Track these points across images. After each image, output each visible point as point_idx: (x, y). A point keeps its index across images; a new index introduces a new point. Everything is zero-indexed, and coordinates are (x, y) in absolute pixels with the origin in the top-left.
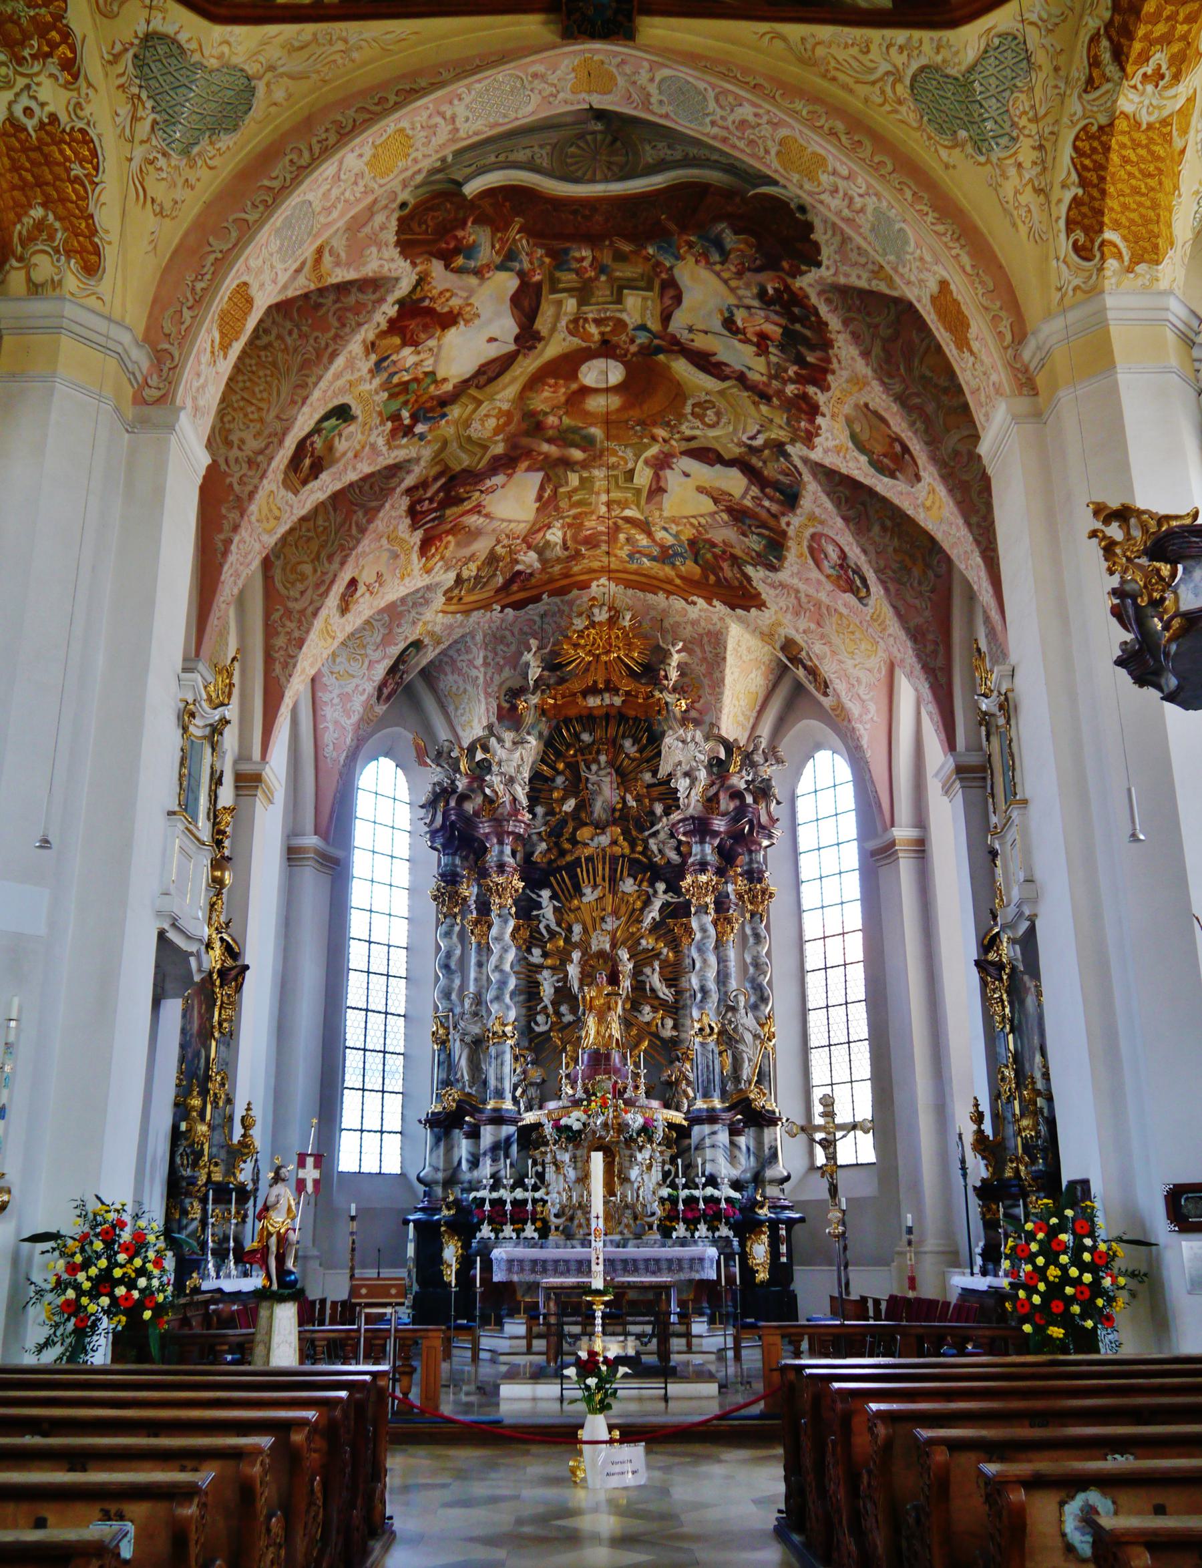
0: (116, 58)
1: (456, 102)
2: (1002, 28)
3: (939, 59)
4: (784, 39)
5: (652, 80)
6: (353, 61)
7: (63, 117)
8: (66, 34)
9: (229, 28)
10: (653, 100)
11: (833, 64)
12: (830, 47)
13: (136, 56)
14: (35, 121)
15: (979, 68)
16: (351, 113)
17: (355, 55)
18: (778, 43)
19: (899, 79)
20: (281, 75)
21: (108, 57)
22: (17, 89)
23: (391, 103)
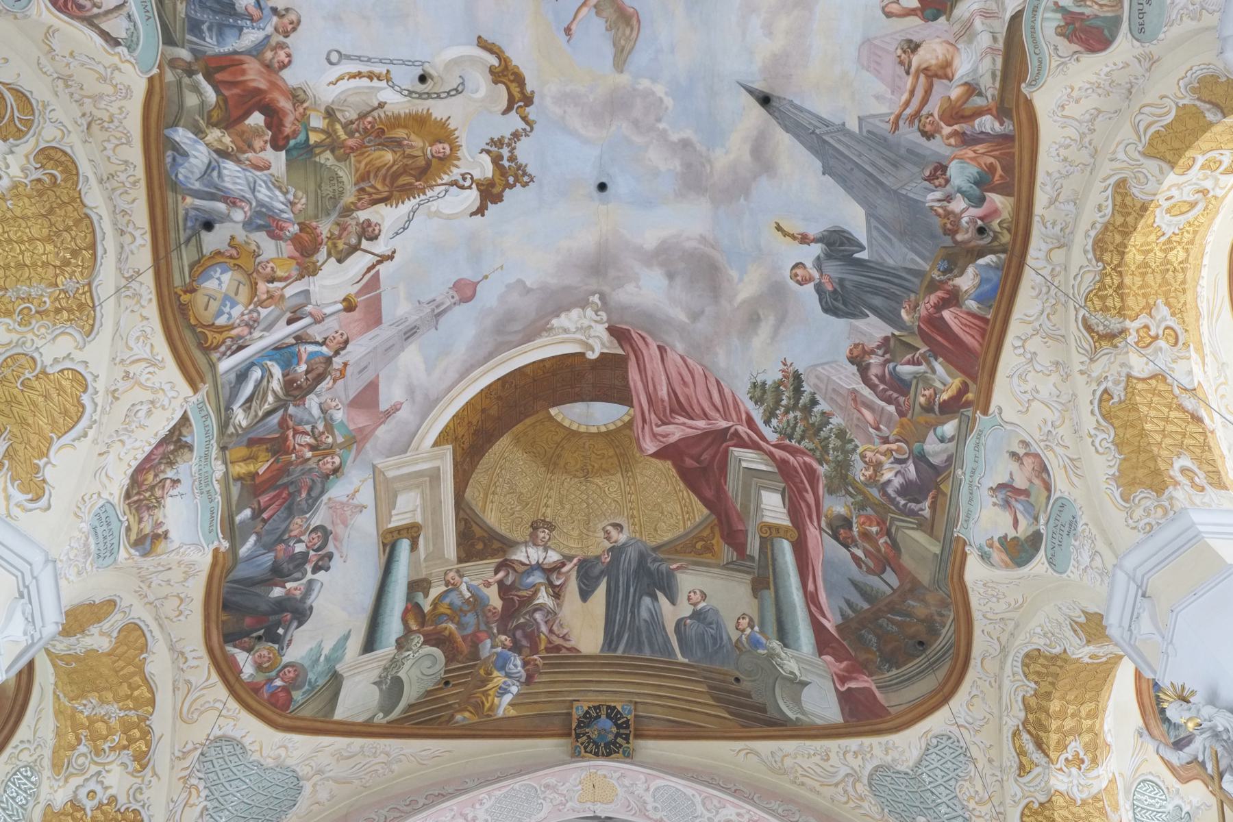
0: (185, 754)
1: (477, 806)
2: (936, 731)
3: (889, 759)
4: (757, 754)
5: (647, 789)
6: (393, 772)
7: (122, 799)
8: (146, 733)
9: (289, 736)
10: (649, 807)
11: (800, 771)
12: (795, 758)
13: (202, 754)
14: (95, 802)
15: (925, 763)
16: (384, 812)
17: (395, 767)
18: (755, 759)
19: (858, 780)
20: (328, 779)
21: (177, 754)
22: (87, 776)
23: (421, 804)
